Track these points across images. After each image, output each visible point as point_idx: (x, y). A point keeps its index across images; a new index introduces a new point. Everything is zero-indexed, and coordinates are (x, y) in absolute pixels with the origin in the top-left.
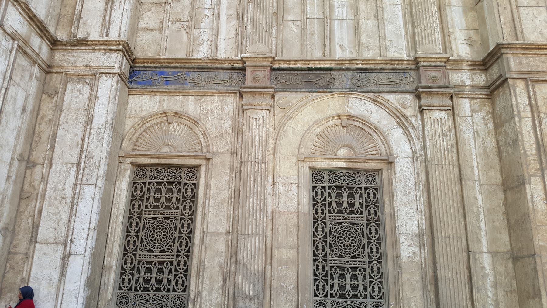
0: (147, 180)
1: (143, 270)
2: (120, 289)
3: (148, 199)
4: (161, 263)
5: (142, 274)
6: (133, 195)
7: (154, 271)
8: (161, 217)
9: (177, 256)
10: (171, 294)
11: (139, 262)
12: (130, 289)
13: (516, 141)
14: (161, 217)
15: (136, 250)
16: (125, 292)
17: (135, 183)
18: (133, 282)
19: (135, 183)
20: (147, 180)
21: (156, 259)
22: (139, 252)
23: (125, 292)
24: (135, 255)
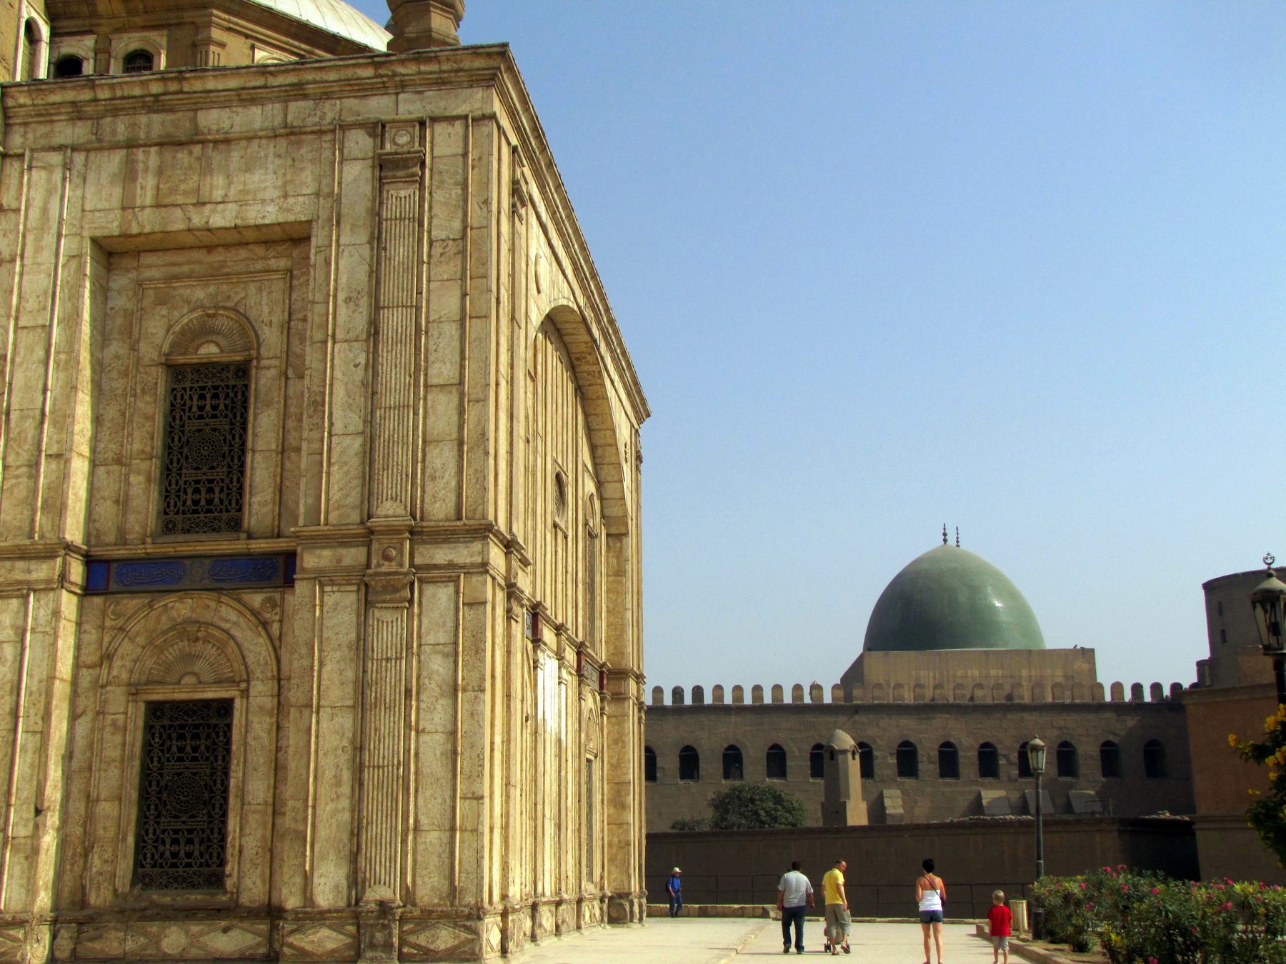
0: (188, 385)
1: (190, 491)
2: (166, 513)
3: (190, 409)
4: (211, 481)
5: (189, 496)
6: (172, 405)
7: (203, 490)
8: (207, 429)
9: (229, 473)
10: (225, 515)
11: (185, 482)
12: (177, 513)
13: (318, 405)
14: (207, 429)
15: (180, 469)
16: (172, 516)
17: (173, 390)
18: (180, 504)
19: (173, 390)
20: (188, 385)
21: (204, 478)
22: (184, 471)
23: (172, 516)
24: (180, 475)
